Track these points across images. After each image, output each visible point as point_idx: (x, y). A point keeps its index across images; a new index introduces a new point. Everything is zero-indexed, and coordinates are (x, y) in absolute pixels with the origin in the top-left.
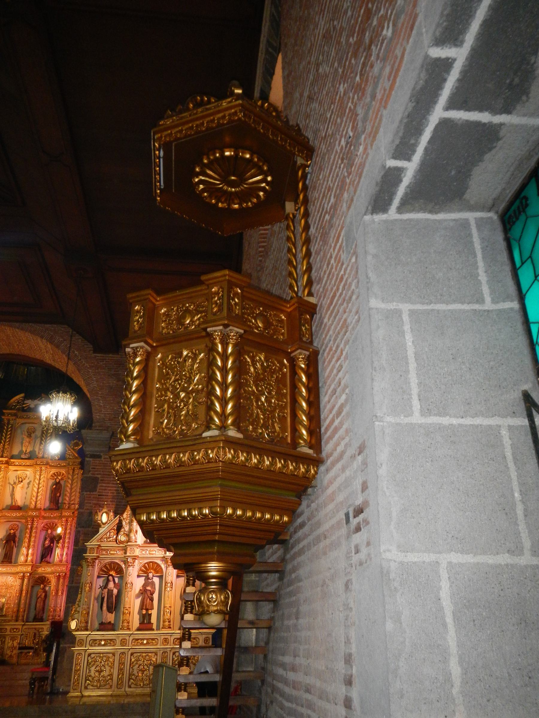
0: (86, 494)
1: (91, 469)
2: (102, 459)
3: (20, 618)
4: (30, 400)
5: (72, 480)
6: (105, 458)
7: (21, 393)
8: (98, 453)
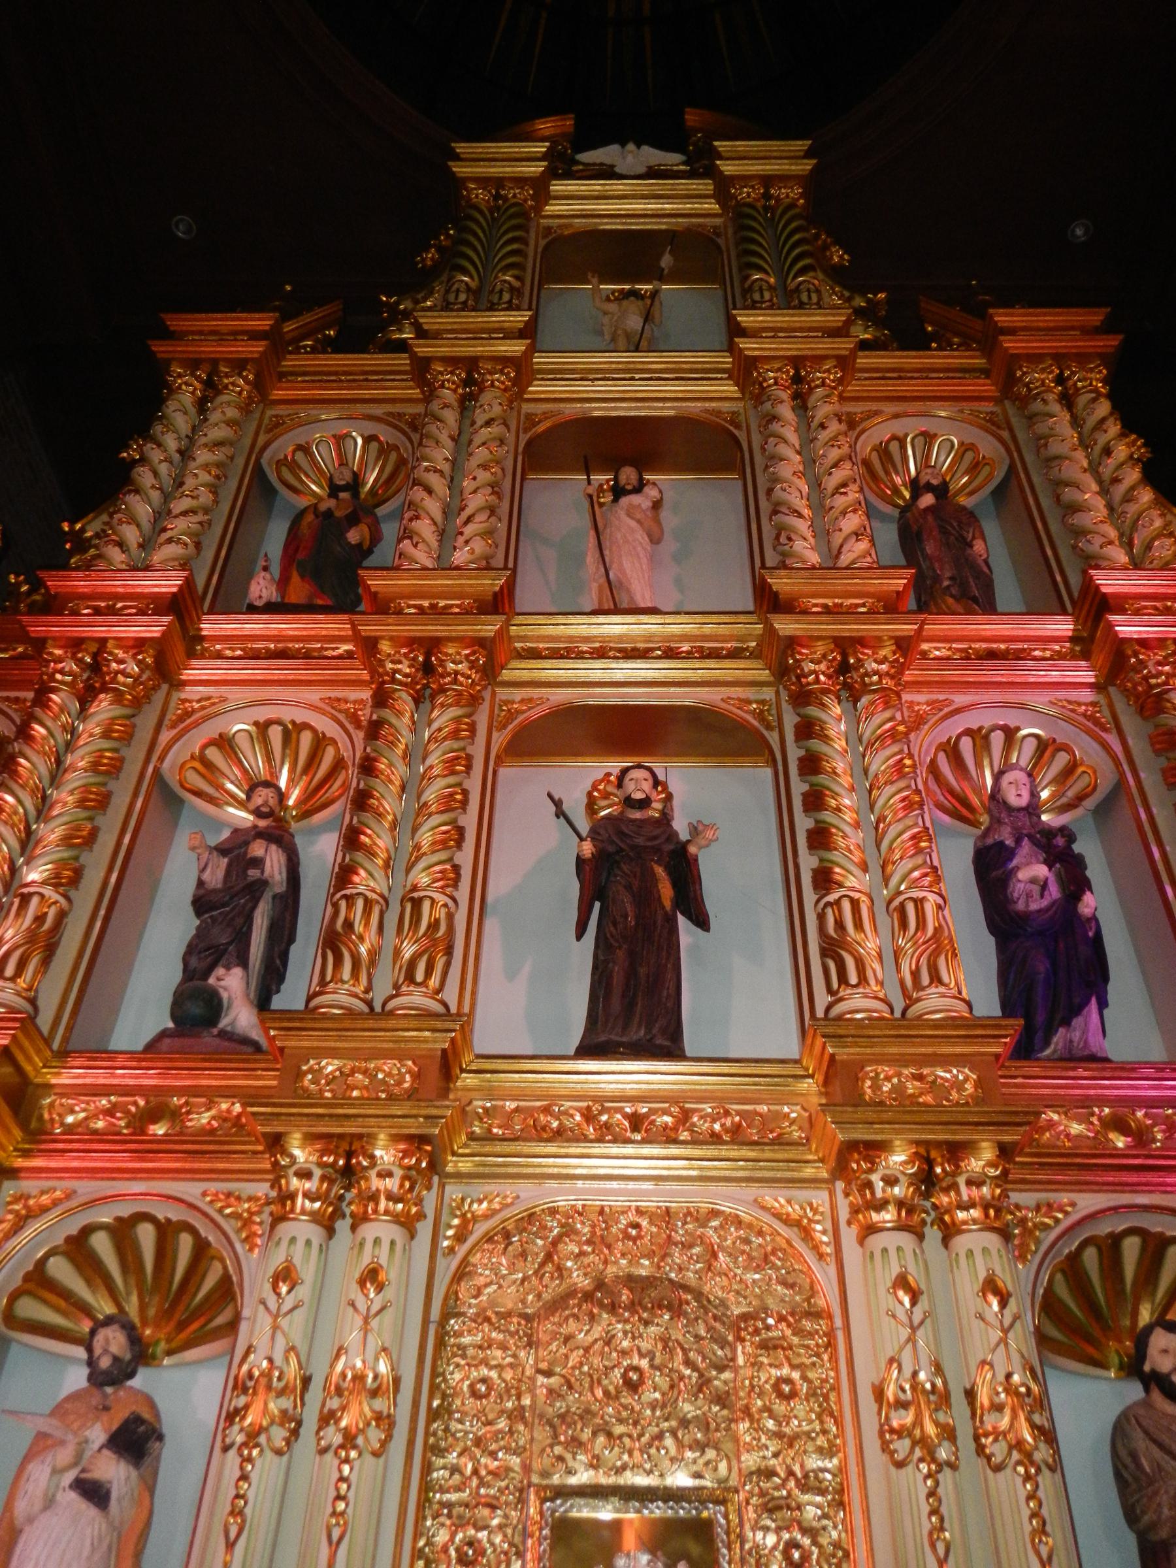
4: (615, 148)
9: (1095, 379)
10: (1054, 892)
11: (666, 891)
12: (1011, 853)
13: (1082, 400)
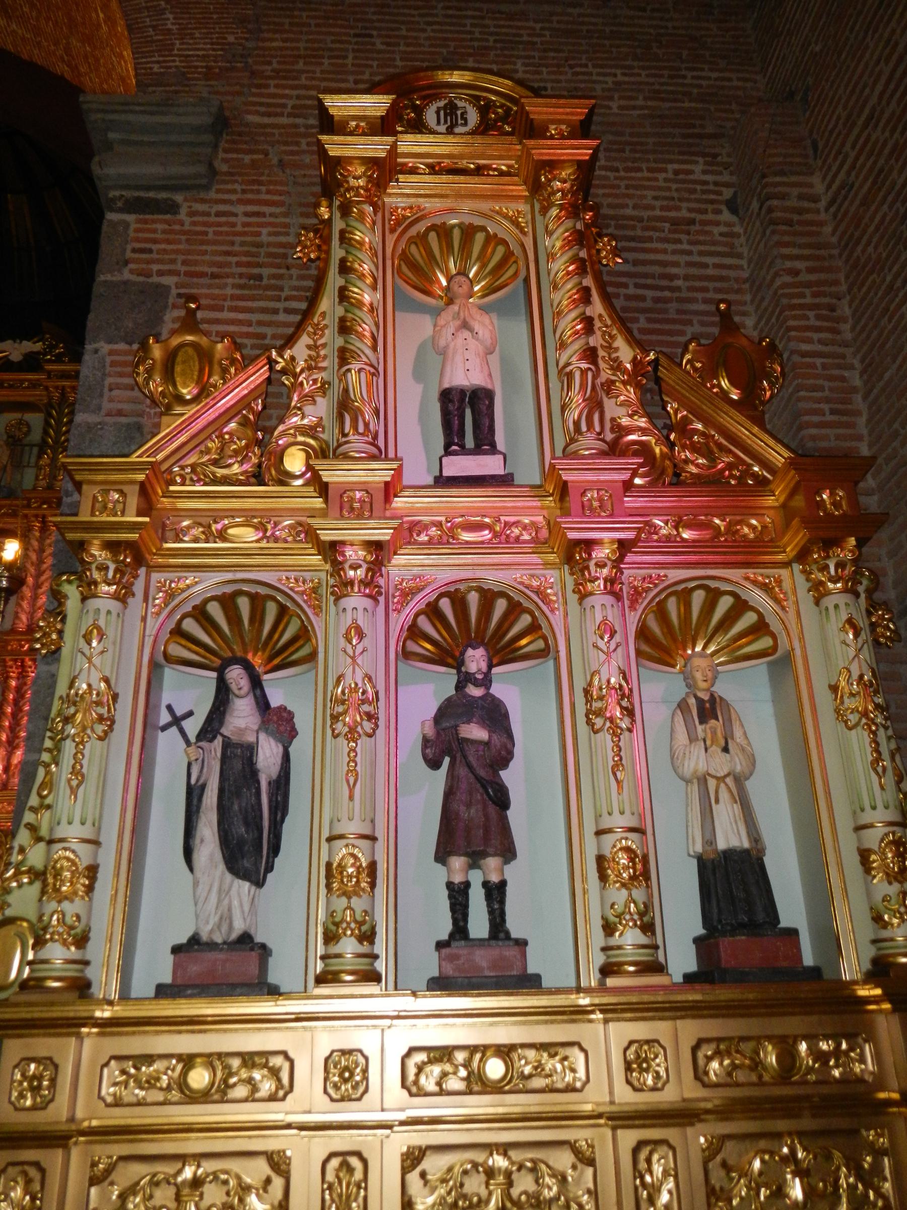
0: (111, 353)
1: (129, 254)
2: (183, 215)
6: (191, 214)
8: (163, 195)
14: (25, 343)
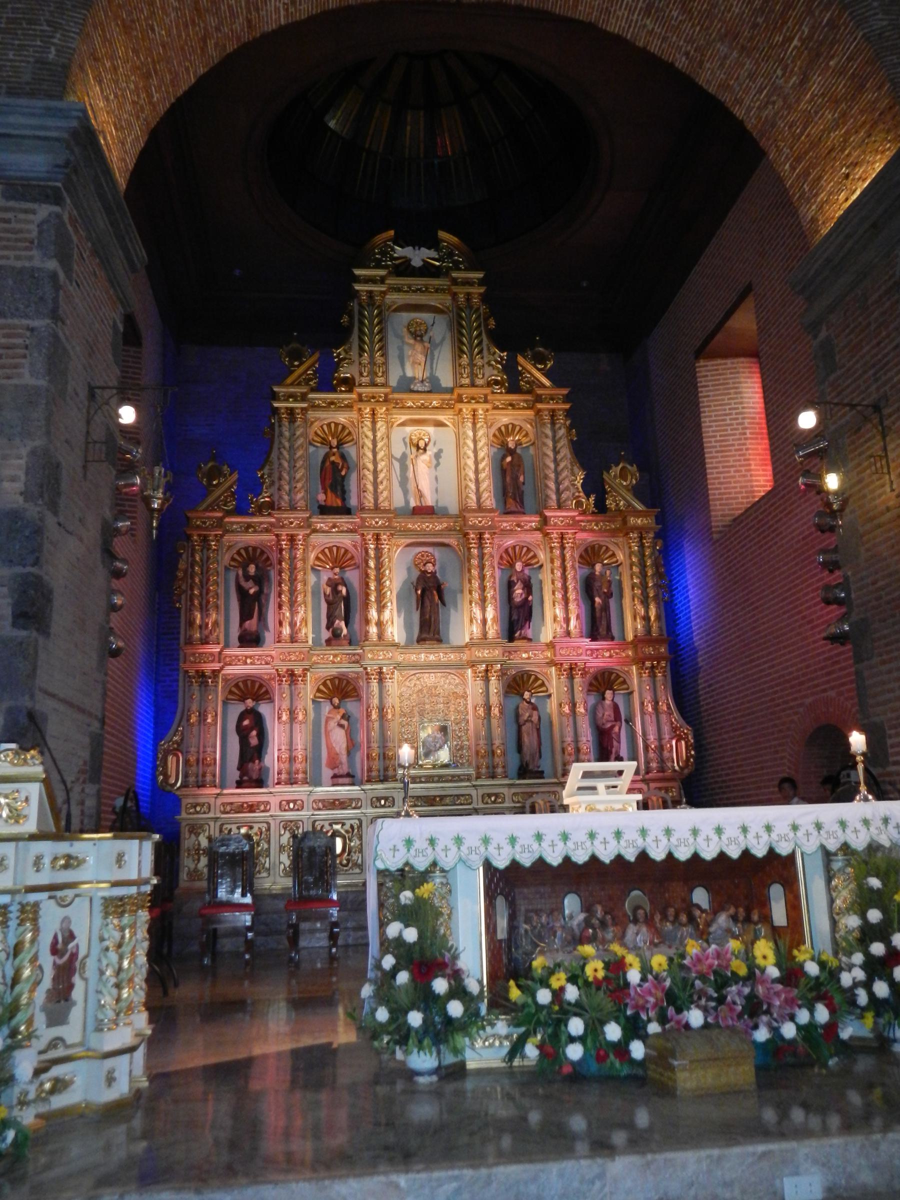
3: (499, 770)
4: (410, 248)
5: (555, 441)
7: (387, 229)
9: (561, 419)
10: (524, 596)
11: (437, 597)
12: (515, 584)
13: (557, 426)
14: (422, 249)
